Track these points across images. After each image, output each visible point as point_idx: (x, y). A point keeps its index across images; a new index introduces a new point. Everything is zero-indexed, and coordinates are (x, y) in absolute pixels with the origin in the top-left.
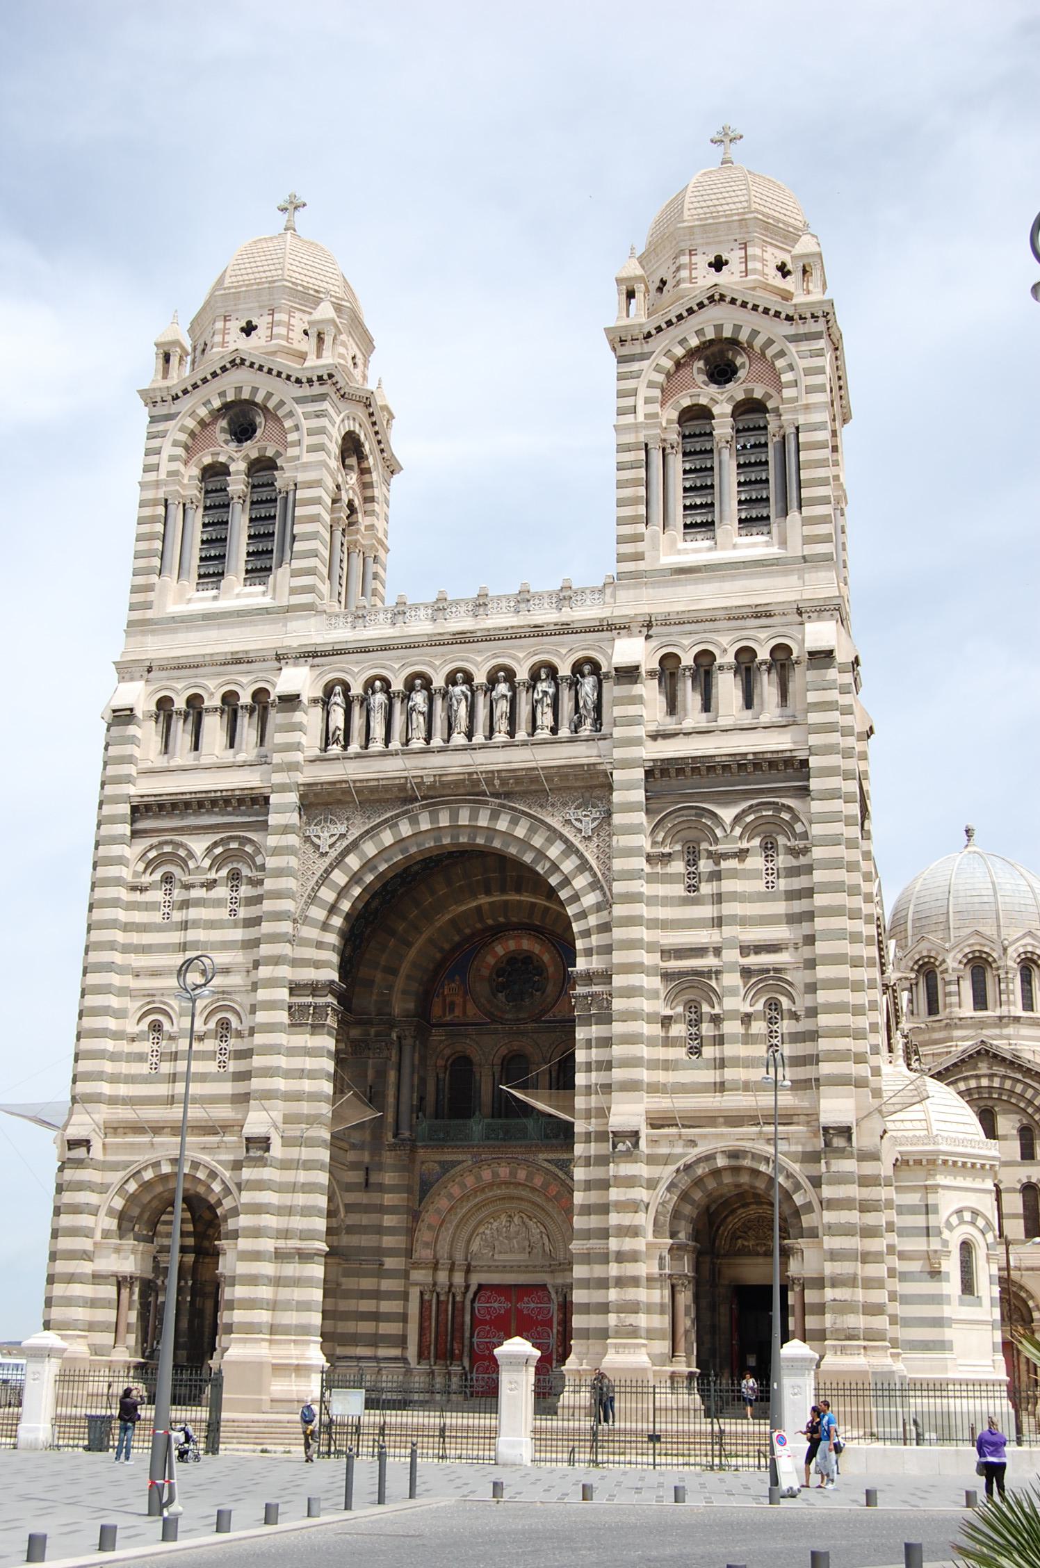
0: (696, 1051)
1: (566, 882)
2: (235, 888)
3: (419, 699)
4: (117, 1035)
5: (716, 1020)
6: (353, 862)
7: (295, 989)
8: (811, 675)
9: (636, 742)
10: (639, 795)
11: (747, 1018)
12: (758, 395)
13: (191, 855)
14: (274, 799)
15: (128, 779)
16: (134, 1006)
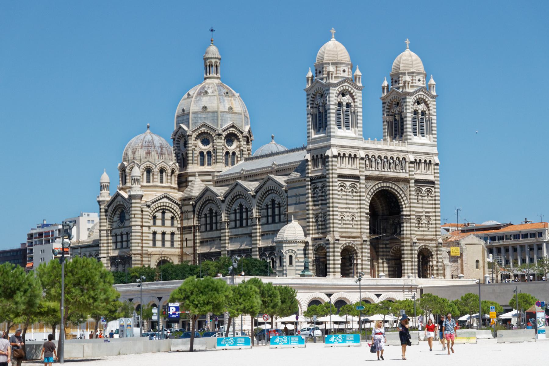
0: (418, 229)
1: (402, 198)
2: (352, 193)
3: (379, 161)
4: (337, 219)
5: (422, 224)
6: (372, 191)
7: (367, 214)
8: (436, 167)
9: (413, 175)
10: (413, 185)
11: (426, 224)
12: (425, 110)
13: (346, 186)
14: (361, 177)
15: (336, 170)
16: (339, 214)
